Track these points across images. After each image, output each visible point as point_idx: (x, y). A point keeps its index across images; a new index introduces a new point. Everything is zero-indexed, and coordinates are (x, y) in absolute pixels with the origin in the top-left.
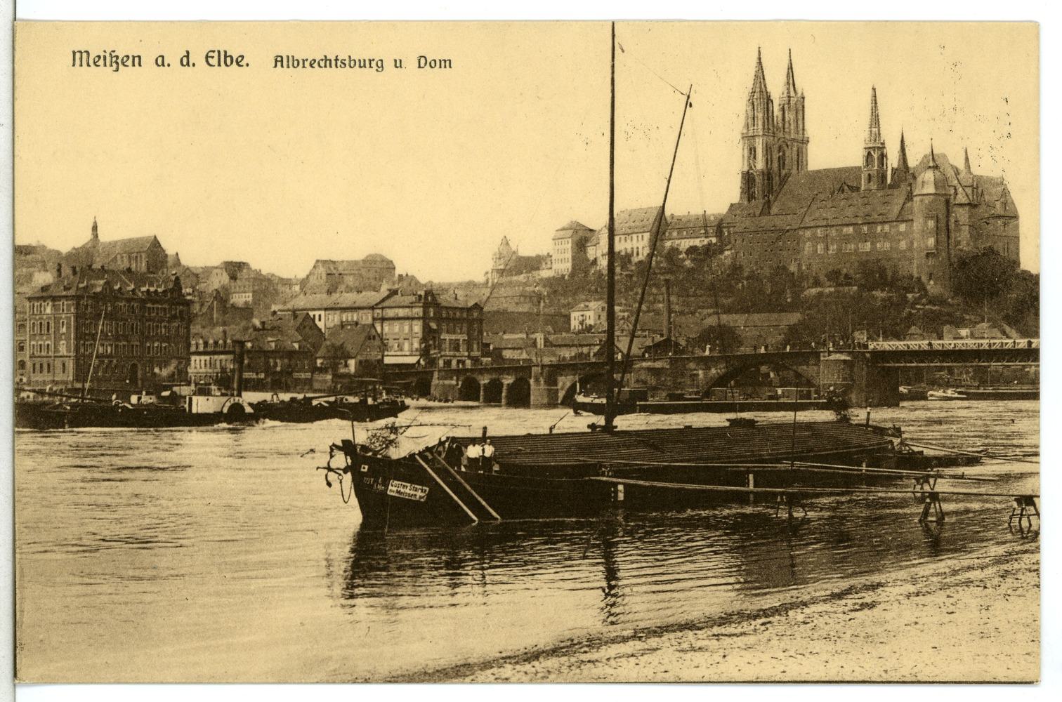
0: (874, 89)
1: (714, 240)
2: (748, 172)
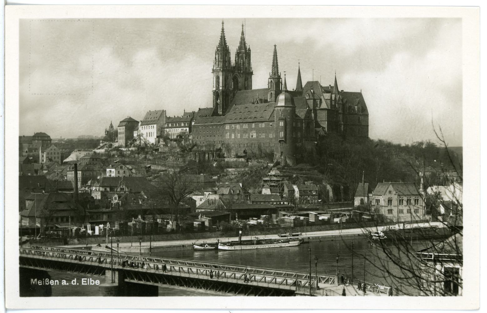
0: (275, 46)
1: (188, 129)
2: (215, 91)
